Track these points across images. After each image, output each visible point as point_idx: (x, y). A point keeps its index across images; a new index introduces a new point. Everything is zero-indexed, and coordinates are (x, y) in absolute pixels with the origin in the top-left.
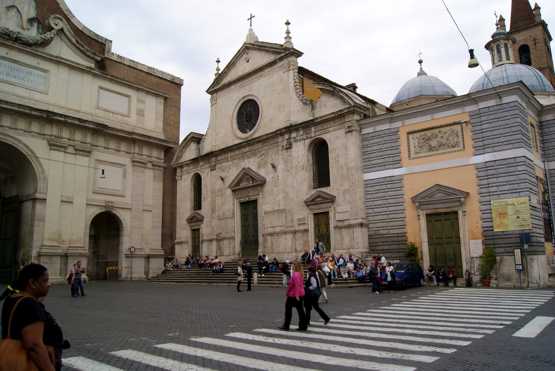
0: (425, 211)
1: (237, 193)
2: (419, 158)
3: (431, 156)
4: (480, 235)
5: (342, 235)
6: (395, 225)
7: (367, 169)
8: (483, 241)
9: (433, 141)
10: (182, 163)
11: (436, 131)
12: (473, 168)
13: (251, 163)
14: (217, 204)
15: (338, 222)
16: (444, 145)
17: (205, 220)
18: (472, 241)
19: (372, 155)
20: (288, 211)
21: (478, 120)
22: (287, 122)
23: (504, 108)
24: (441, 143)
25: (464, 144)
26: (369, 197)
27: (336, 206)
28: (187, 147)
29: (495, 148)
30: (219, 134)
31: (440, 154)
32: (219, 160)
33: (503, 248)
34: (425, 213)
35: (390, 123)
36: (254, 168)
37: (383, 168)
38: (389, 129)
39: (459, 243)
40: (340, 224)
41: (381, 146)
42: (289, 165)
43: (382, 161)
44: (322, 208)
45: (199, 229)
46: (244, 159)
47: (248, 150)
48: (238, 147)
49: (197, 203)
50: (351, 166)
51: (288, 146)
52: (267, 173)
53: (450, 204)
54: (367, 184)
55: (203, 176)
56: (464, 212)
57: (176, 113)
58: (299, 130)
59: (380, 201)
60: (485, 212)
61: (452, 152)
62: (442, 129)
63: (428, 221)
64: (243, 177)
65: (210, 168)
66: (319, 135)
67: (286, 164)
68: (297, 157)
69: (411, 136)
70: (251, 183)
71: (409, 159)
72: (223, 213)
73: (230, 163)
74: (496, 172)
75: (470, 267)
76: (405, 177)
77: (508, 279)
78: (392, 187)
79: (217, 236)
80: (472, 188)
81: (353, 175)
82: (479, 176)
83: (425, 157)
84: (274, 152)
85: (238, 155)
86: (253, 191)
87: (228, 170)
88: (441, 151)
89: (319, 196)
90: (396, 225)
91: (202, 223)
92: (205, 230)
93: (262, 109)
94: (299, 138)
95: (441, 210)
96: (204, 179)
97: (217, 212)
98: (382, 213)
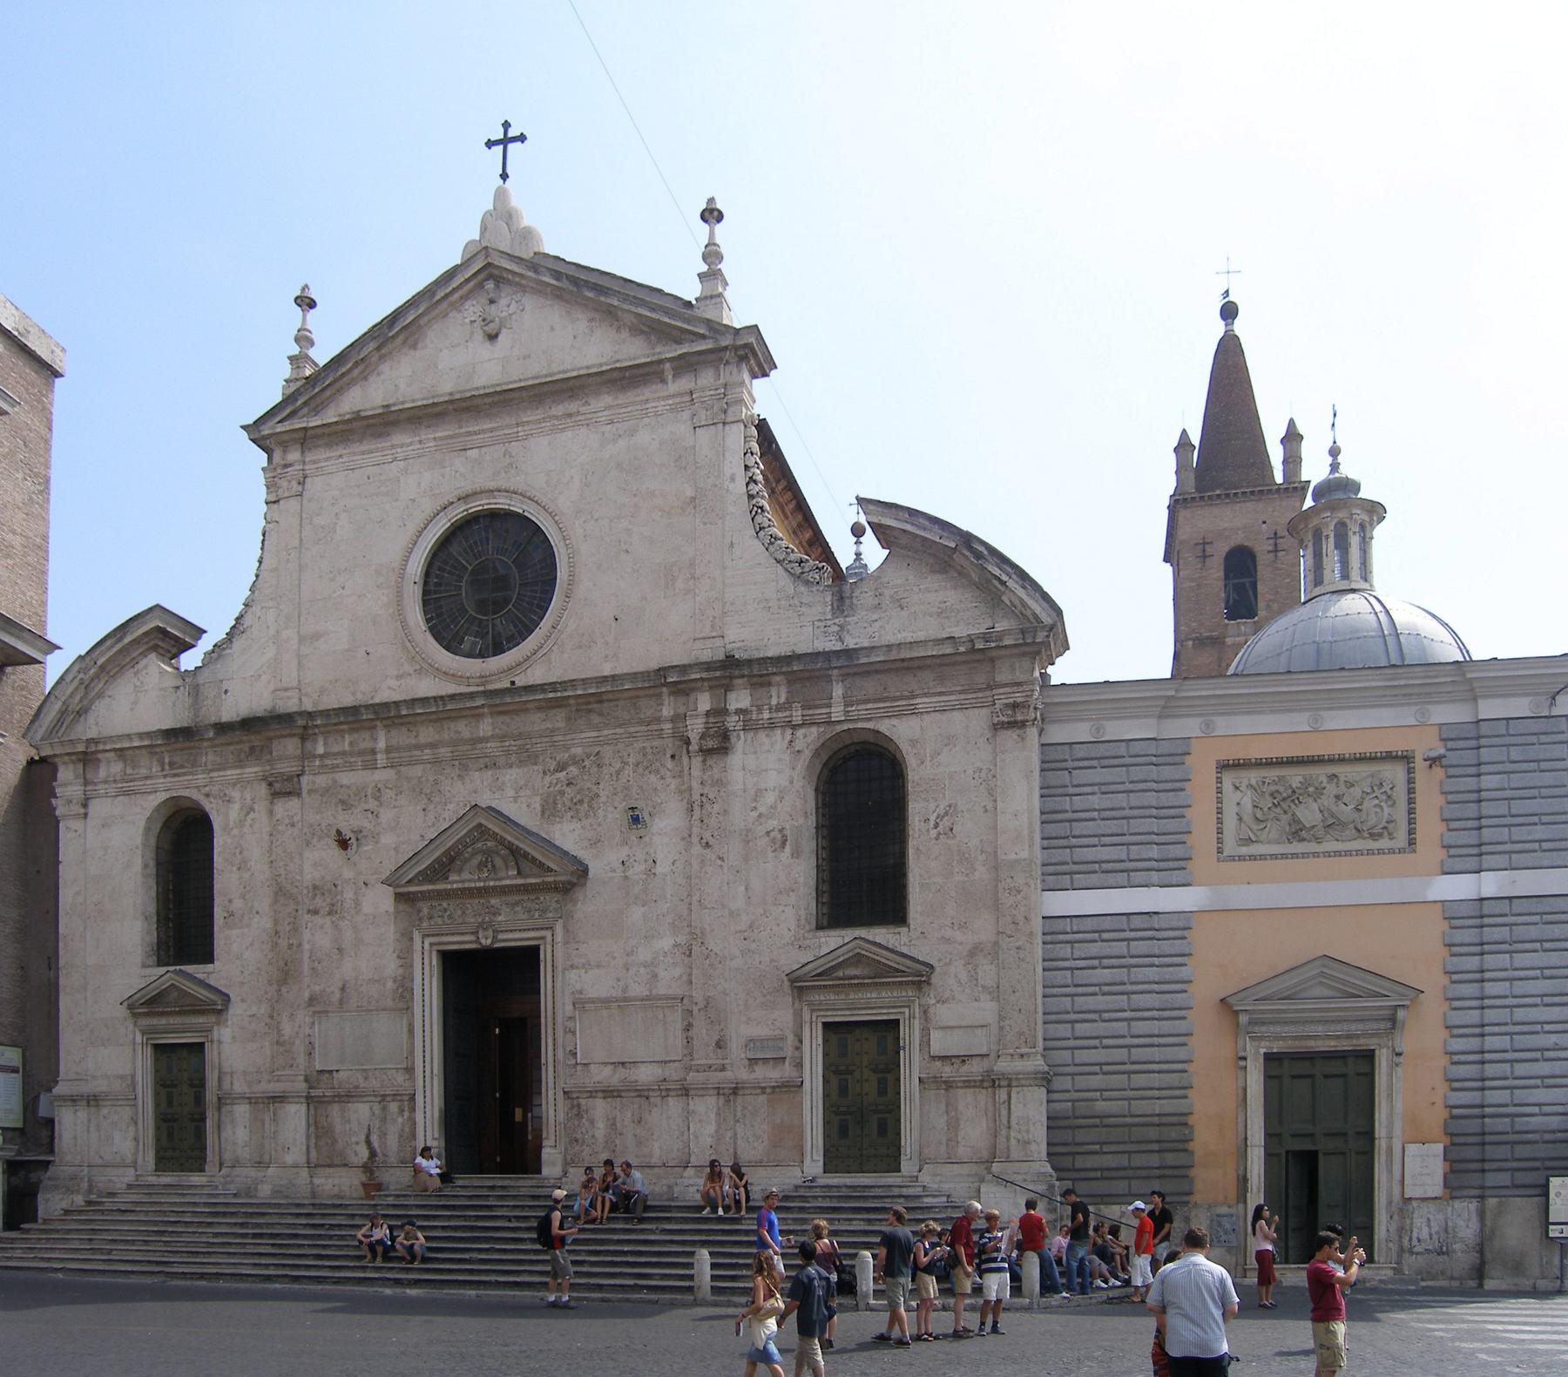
0: (1263, 1044)
1: (425, 911)
2: (1253, 858)
3: (1295, 856)
4: (1437, 1131)
5: (956, 1110)
6: (1152, 1086)
7: (1059, 876)
9: (1306, 808)
11: (1320, 773)
14: (306, 947)
15: (938, 1064)
16: (1343, 825)
17: (237, 1011)
18: (1412, 1149)
19: (1079, 828)
20: (701, 1005)
21: (1469, 757)
22: (709, 643)
23: (1555, 730)
24: (1333, 815)
25: (1411, 832)
26: (1060, 981)
27: (933, 1001)
29: (1514, 856)
30: (317, 636)
31: (1327, 854)
32: (322, 757)
33: (1509, 1173)
34: (1262, 1051)
35: (1160, 717)
36: (523, 812)
38: (1154, 739)
39: (1368, 1154)
40: (947, 1071)
41: (1121, 800)
42: (713, 822)
43: (1120, 853)
44: (871, 1005)
46: (465, 768)
47: (490, 734)
49: (171, 934)
50: (1013, 856)
51: (710, 744)
52: (595, 843)
53: (1353, 1027)
56: (1398, 1054)
58: (770, 684)
59: (1100, 998)
60: (1463, 1058)
61: (1370, 852)
62: (1343, 771)
63: (1269, 1077)
64: (466, 847)
65: (270, 784)
66: (870, 719)
67: (697, 813)
68: (753, 792)
69: (1228, 779)
70: (510, 878)
71: (1218, 860)
72: (343, 989)
74: (1511, 936)
75: (1397, 1230)
77: (1517, 1268)
78: (1152, 953)
79: (306, 1080)
80: (1428, 975)
81: (1019, 892)
82: (1456, 941)
83: (1274, 857)
84: (631, 760)
85: (433, 746)
86: (518, 909)
89: (857, 959)
90: (1157, 1085)
91: (218, 1024)
93: (571, 565)
94: (766, 715)
95: (1320, 1043)
96: (226, 829)
97: (306, 980)
98: (1106, 1042)
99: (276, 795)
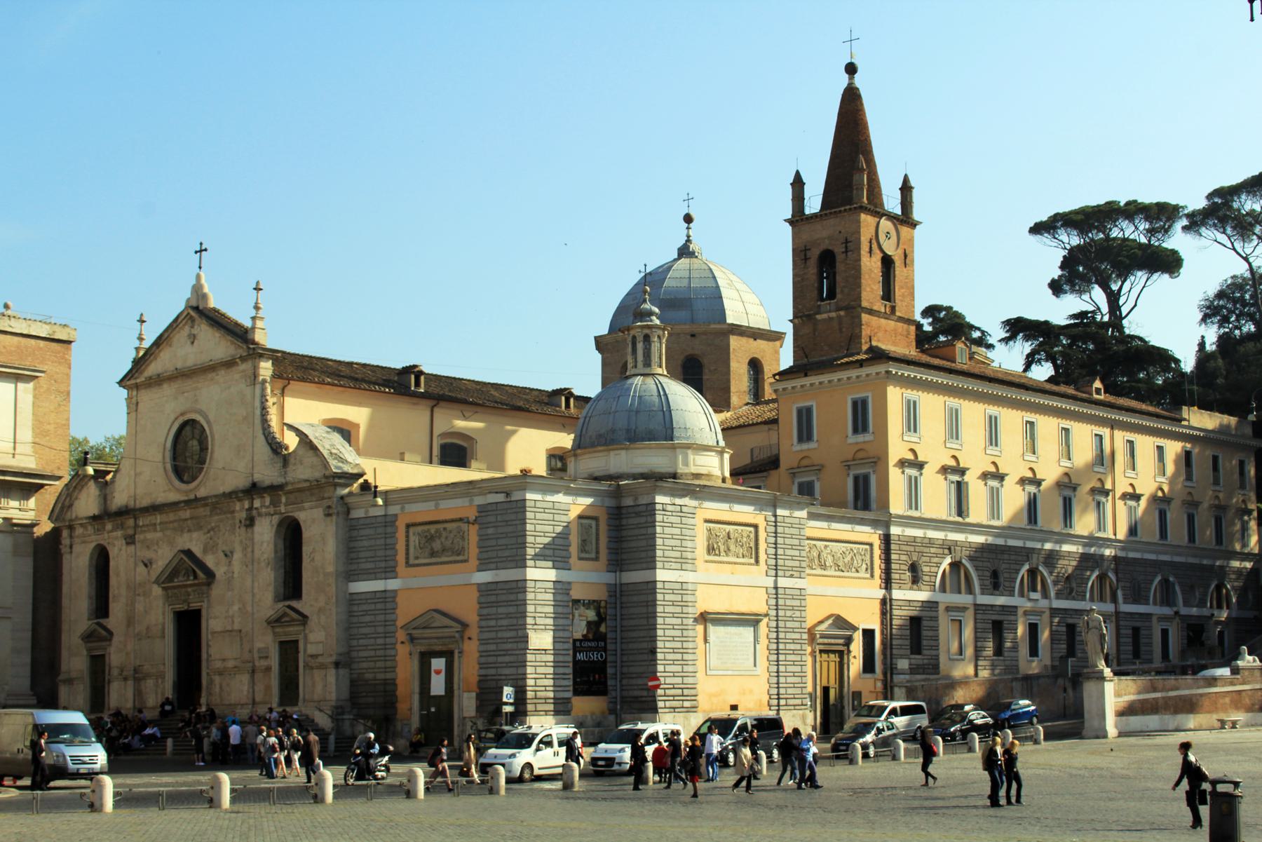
4: (475, 687)
8: (477, 695)
11: (440, 526)
13: (194, 542)
15: (310, 659)
17: (115, 640)
18: (466, 695)
28: (82, 487)
30: (140, 474)
32: (141, 527)
36: (197, 551)
45: (103, 656)
51: (248, 522)
54: (353, 601)
55: (113, 552)
57: (59, 405)
65: (125, 539)
69: (412, 530)
73: (159, 535)
76: (400, 594)
80: (471, 617)
87: (156, 547)
92: (116, 657)
99: (128, 544)
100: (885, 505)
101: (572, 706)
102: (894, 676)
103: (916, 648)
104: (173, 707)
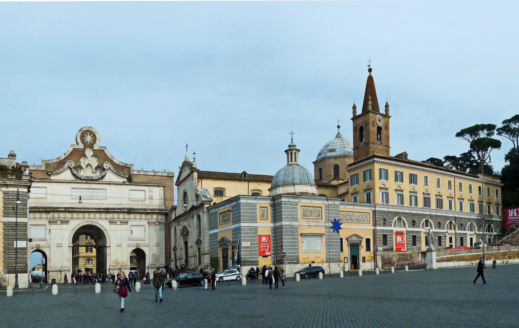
7: (211, 229)
10: (171, 221)
11: (225, 213)
12: (231, 230)
13: (186, 224)
37: (213, 229)
48: (157, 225)
69: (220, 215)
76: (219, 233)
88: (226, 222)
100: (374, 201)
101: (259, 263)
102: (377, 252)
103: (385, 243)
104: (184, 266)
